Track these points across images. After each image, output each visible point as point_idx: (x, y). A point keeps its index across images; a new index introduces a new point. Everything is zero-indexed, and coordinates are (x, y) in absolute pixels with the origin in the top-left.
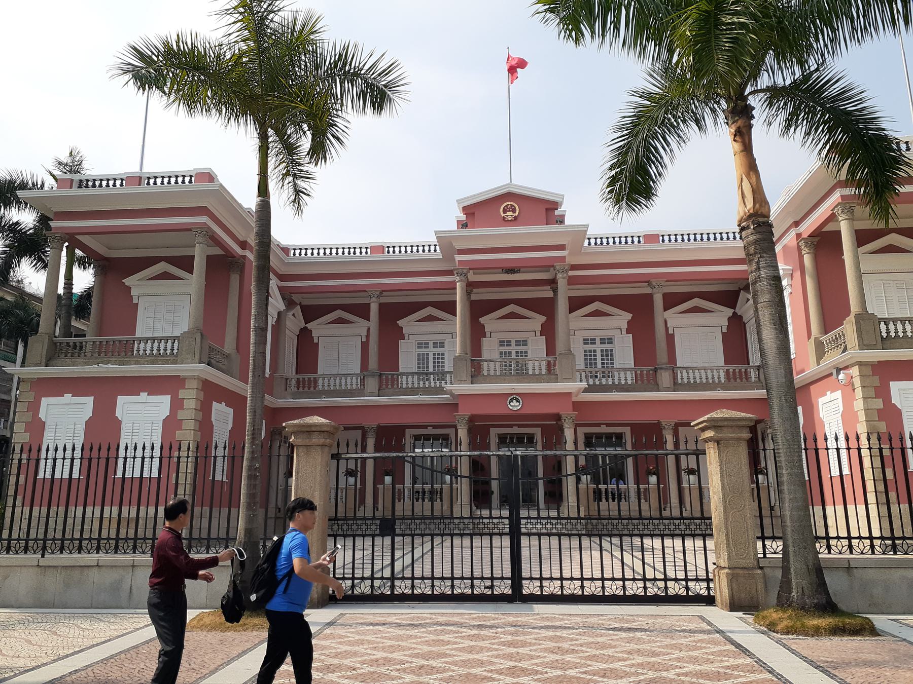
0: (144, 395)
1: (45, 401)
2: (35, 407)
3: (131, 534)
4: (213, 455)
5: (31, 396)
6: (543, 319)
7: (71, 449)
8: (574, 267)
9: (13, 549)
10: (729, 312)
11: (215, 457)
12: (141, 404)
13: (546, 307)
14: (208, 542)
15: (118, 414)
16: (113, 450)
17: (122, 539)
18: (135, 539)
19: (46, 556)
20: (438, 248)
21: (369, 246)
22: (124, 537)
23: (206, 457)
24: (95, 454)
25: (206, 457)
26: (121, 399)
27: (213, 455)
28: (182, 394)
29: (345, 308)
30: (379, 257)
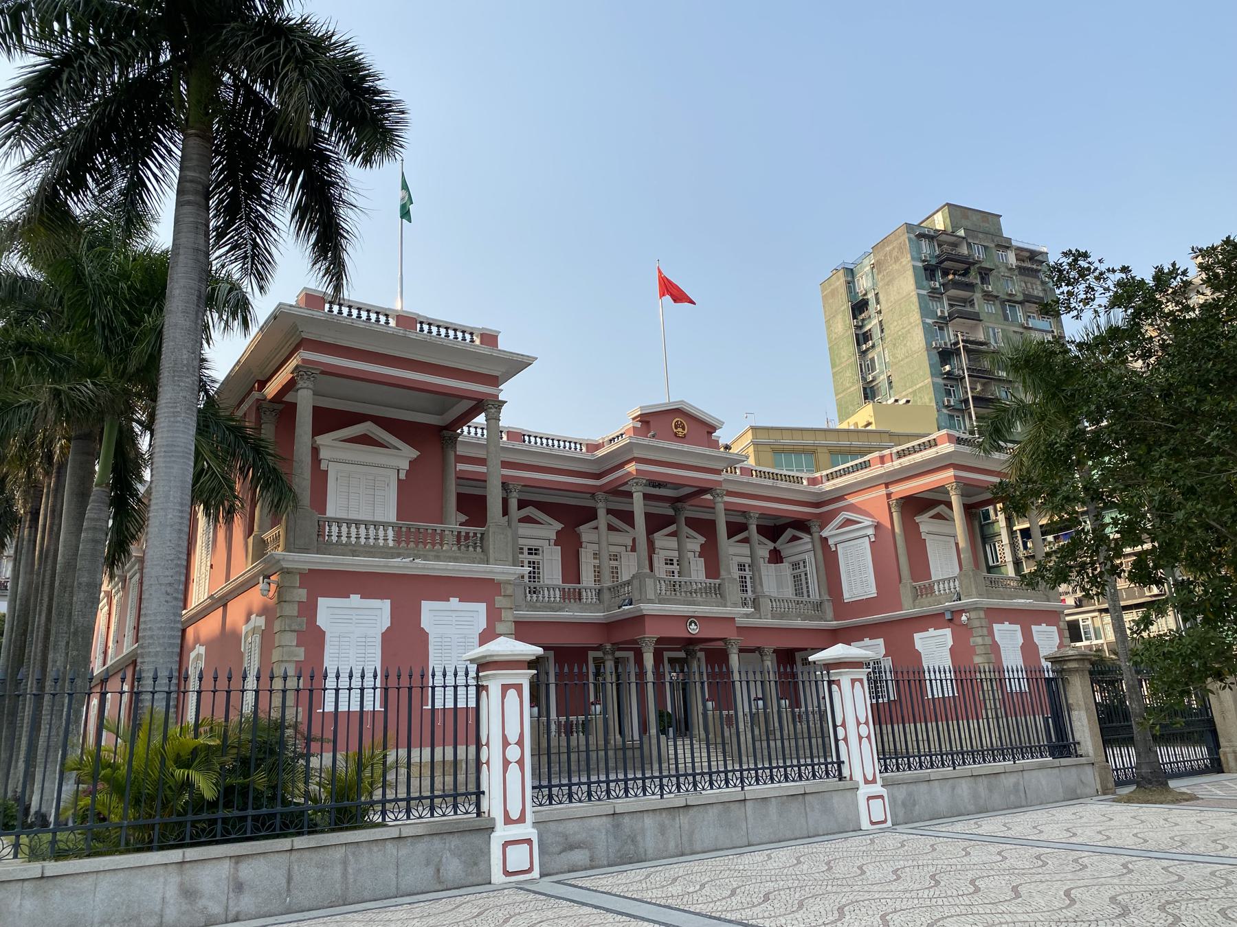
0: (454, 601)
1: (323, 602)
2: (310, 610)
3: (402, 794)
4: (431, 684)
5: (302, 594)
6: (702, 540)
7: (441, 674)
8: (730, 494)
9: (575, 796)
10: (771, 545)
11: (433, 688)
12: (449, 614)
13: (706, 527)
14: (408, 803)
15: (425, 623)
16: (237, 678)
17: (415, 799)
18: (408, 800)
19: (746, 788)
20: (485, 431)
21: (584, 442)
22: (417, 795)
23: (422, 688)
24: (393, 682)
25: (422, 688)
26: (427, 606)
27: (431, 684)
28: (500, 601)
29: (540, 506)
30: (518, 445)
